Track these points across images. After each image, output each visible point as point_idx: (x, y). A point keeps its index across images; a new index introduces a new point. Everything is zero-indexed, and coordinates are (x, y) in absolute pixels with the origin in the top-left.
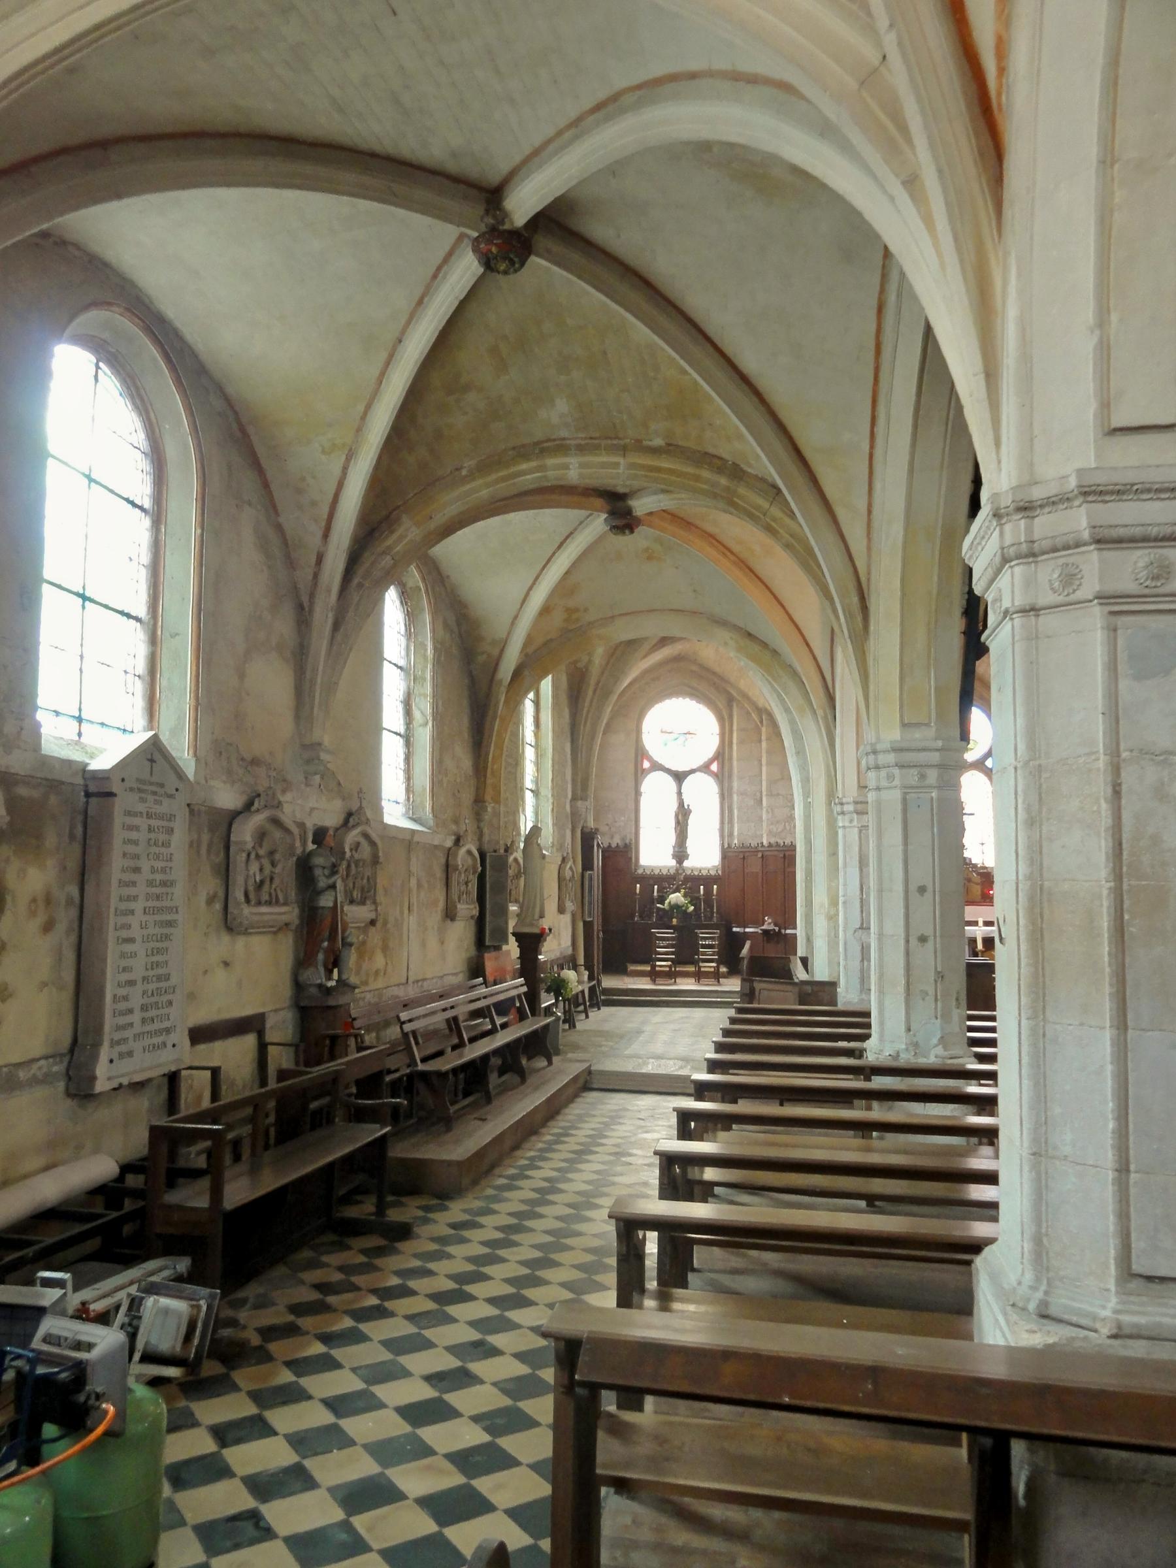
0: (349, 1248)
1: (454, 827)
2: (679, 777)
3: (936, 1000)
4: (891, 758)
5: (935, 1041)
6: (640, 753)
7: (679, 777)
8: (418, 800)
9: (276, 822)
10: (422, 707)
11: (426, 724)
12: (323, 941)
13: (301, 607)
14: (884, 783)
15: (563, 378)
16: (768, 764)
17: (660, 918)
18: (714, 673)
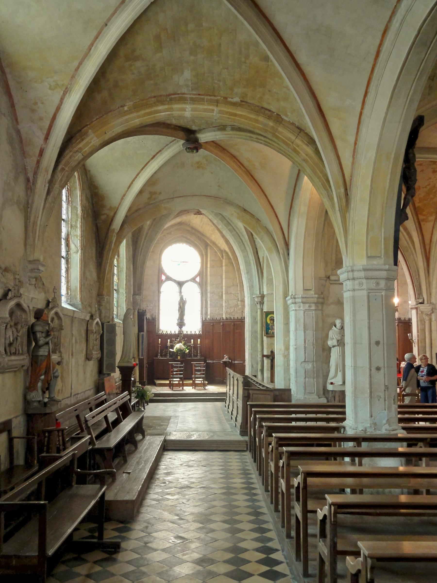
0: (85, 561)
1: (89, 309)
2: (180, 284)
3: (385, 400)
4: (362, 274)
5: (384, 422)
6: (160, 271)
7: (180, 284)
8: (73, 294)
9: (18, 305)
10: (75, 242)
11: (78, 251)
12: (41, 375)
13: (28, 180)
14: (357, 287)
15: (192, 58)
16: (226, 278)
17: (171, 356)
18: (199, 232)
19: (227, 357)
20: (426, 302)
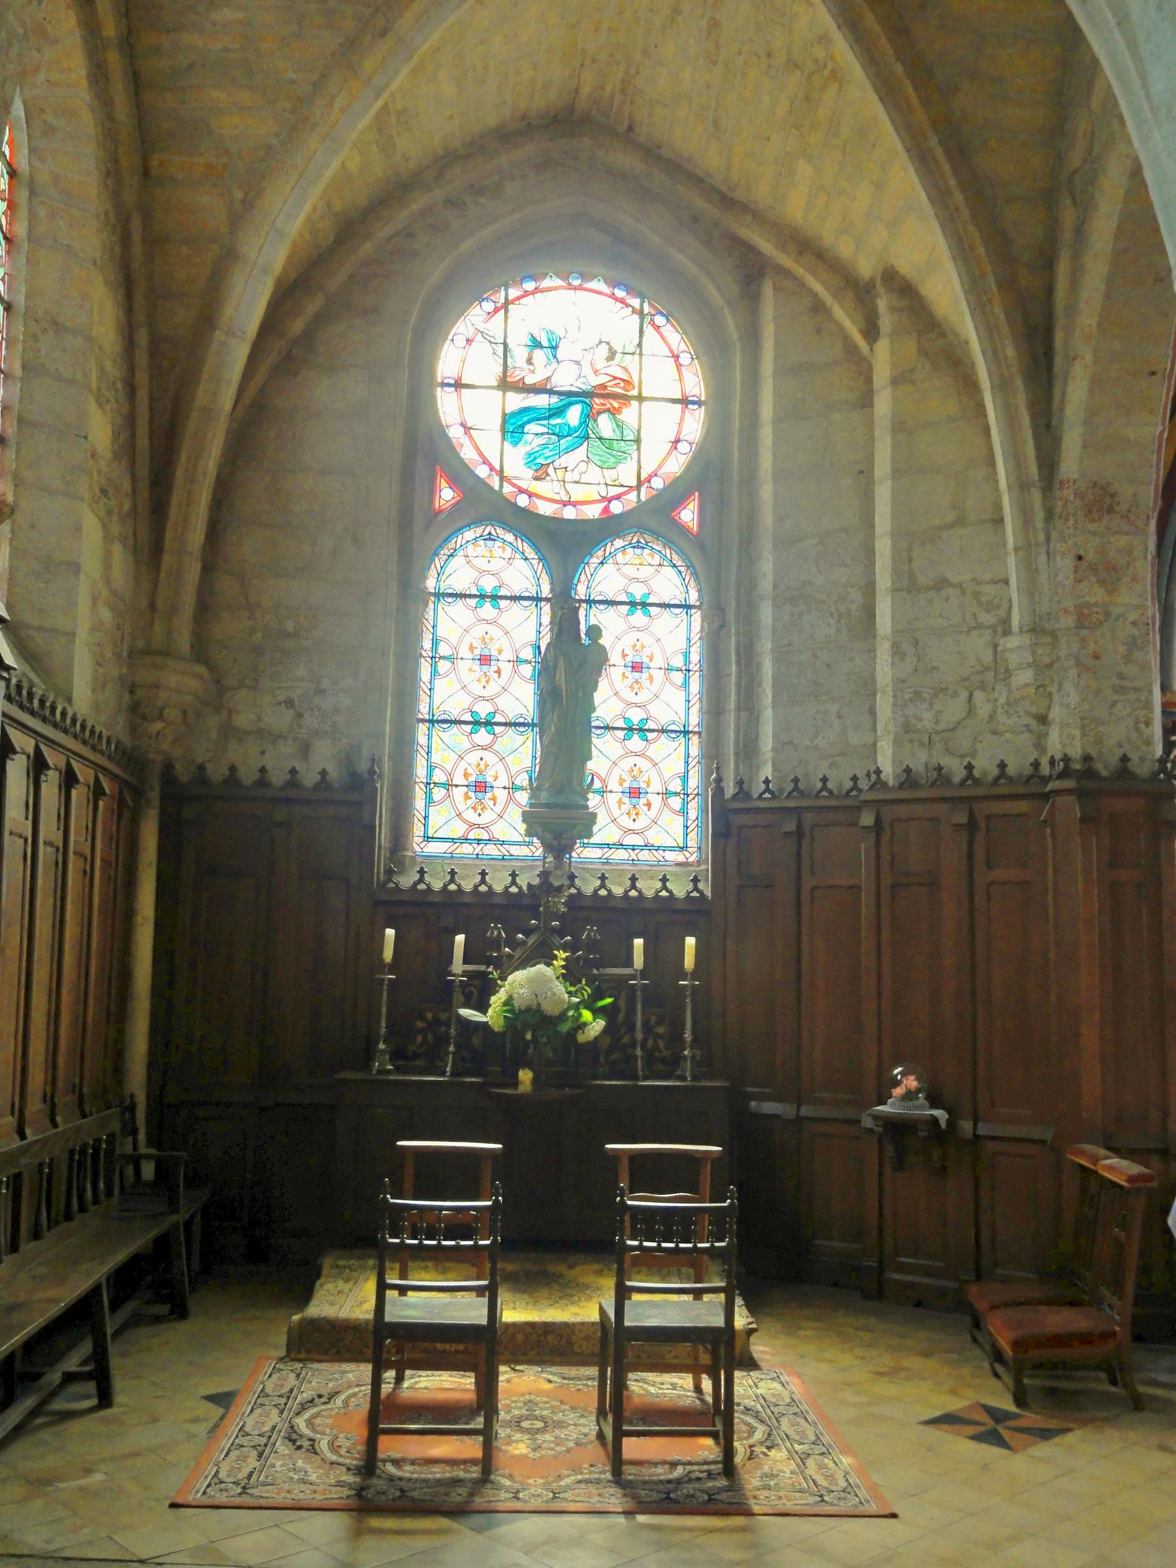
2: (565, 544)
6: (424, 449)
19: (912, 1082)
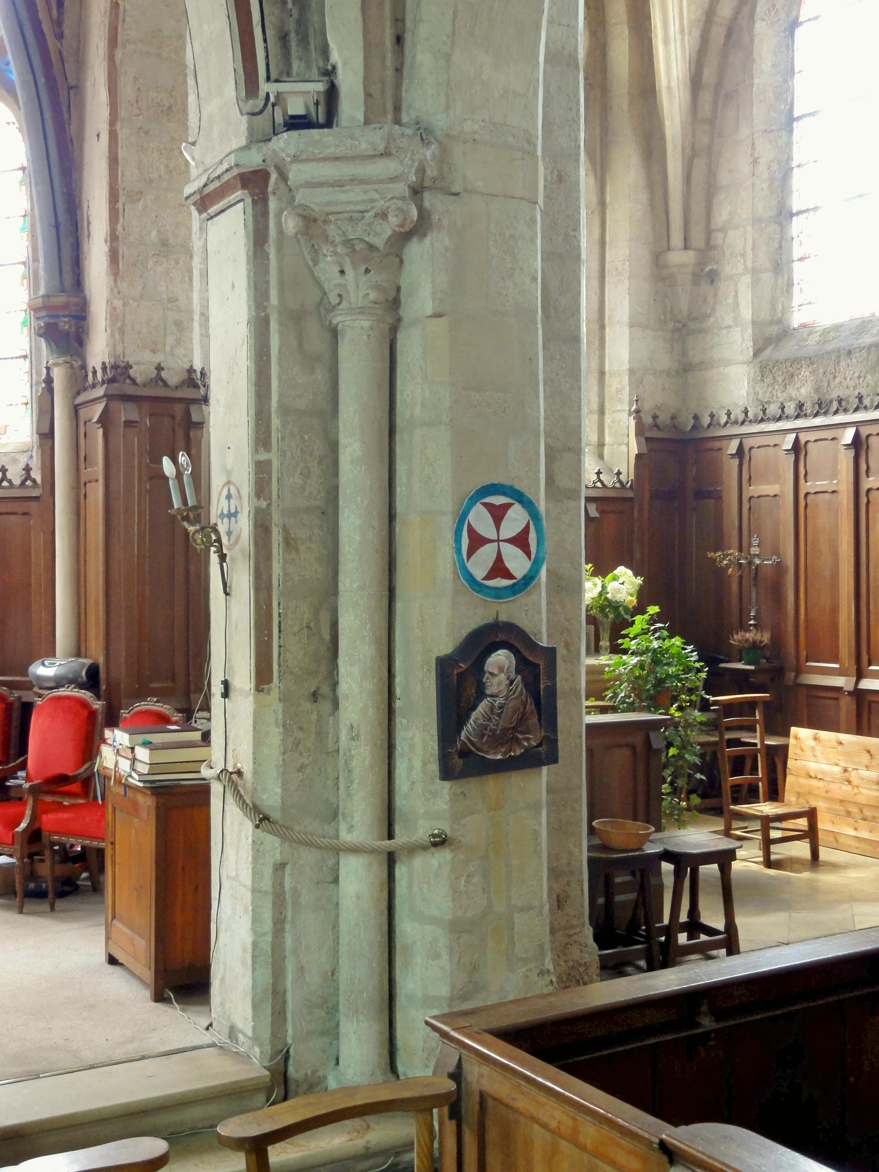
20: (351, 107)
